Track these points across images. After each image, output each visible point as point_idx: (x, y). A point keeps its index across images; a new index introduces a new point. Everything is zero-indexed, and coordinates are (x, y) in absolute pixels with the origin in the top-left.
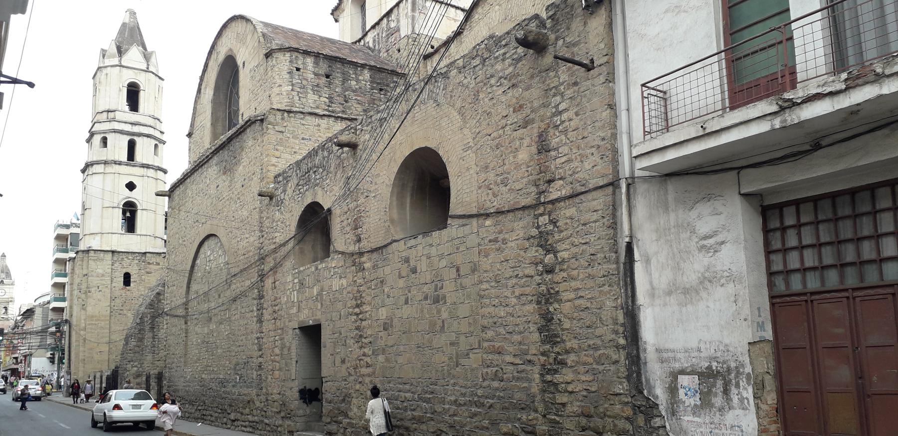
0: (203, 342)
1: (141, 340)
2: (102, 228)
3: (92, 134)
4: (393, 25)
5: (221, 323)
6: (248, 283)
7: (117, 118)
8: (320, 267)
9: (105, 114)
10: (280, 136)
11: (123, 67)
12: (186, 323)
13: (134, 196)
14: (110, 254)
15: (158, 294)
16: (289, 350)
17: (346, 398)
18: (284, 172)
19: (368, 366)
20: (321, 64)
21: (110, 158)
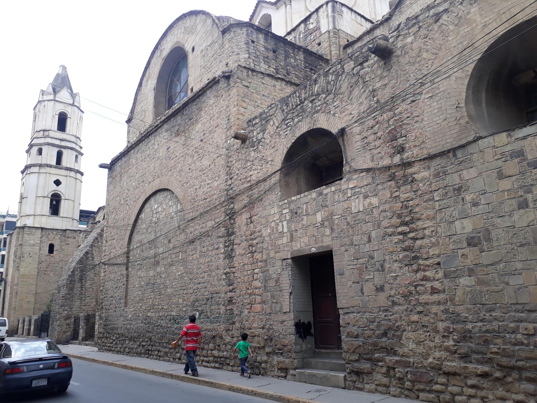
0: (147, 284)
1: (72, 289)
2: (35, 211)
3: (31, 146)
4: (311, 27)
5: (171, 265)
6: (210, 224)
7: (50, 135)
8: (325, 192)
9: (42, 132)
10: (246, 90)
11: (57, 101)
12: (127, 269)
13: (61, 189)
14: (40, 230)
15: (87, 253)
16: (277, 282)
17: (393, 331)
18: (261, 114)
19: (434, 291)
20: (269, 41)
21: (44, 162)
